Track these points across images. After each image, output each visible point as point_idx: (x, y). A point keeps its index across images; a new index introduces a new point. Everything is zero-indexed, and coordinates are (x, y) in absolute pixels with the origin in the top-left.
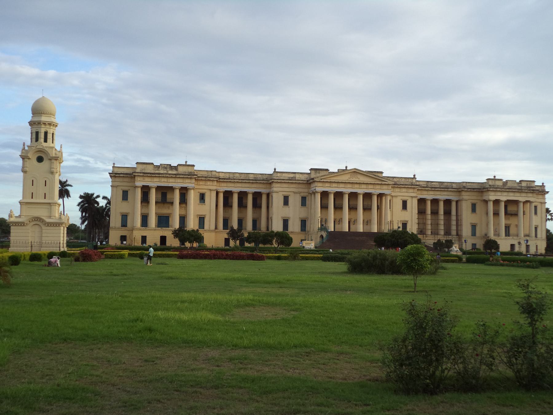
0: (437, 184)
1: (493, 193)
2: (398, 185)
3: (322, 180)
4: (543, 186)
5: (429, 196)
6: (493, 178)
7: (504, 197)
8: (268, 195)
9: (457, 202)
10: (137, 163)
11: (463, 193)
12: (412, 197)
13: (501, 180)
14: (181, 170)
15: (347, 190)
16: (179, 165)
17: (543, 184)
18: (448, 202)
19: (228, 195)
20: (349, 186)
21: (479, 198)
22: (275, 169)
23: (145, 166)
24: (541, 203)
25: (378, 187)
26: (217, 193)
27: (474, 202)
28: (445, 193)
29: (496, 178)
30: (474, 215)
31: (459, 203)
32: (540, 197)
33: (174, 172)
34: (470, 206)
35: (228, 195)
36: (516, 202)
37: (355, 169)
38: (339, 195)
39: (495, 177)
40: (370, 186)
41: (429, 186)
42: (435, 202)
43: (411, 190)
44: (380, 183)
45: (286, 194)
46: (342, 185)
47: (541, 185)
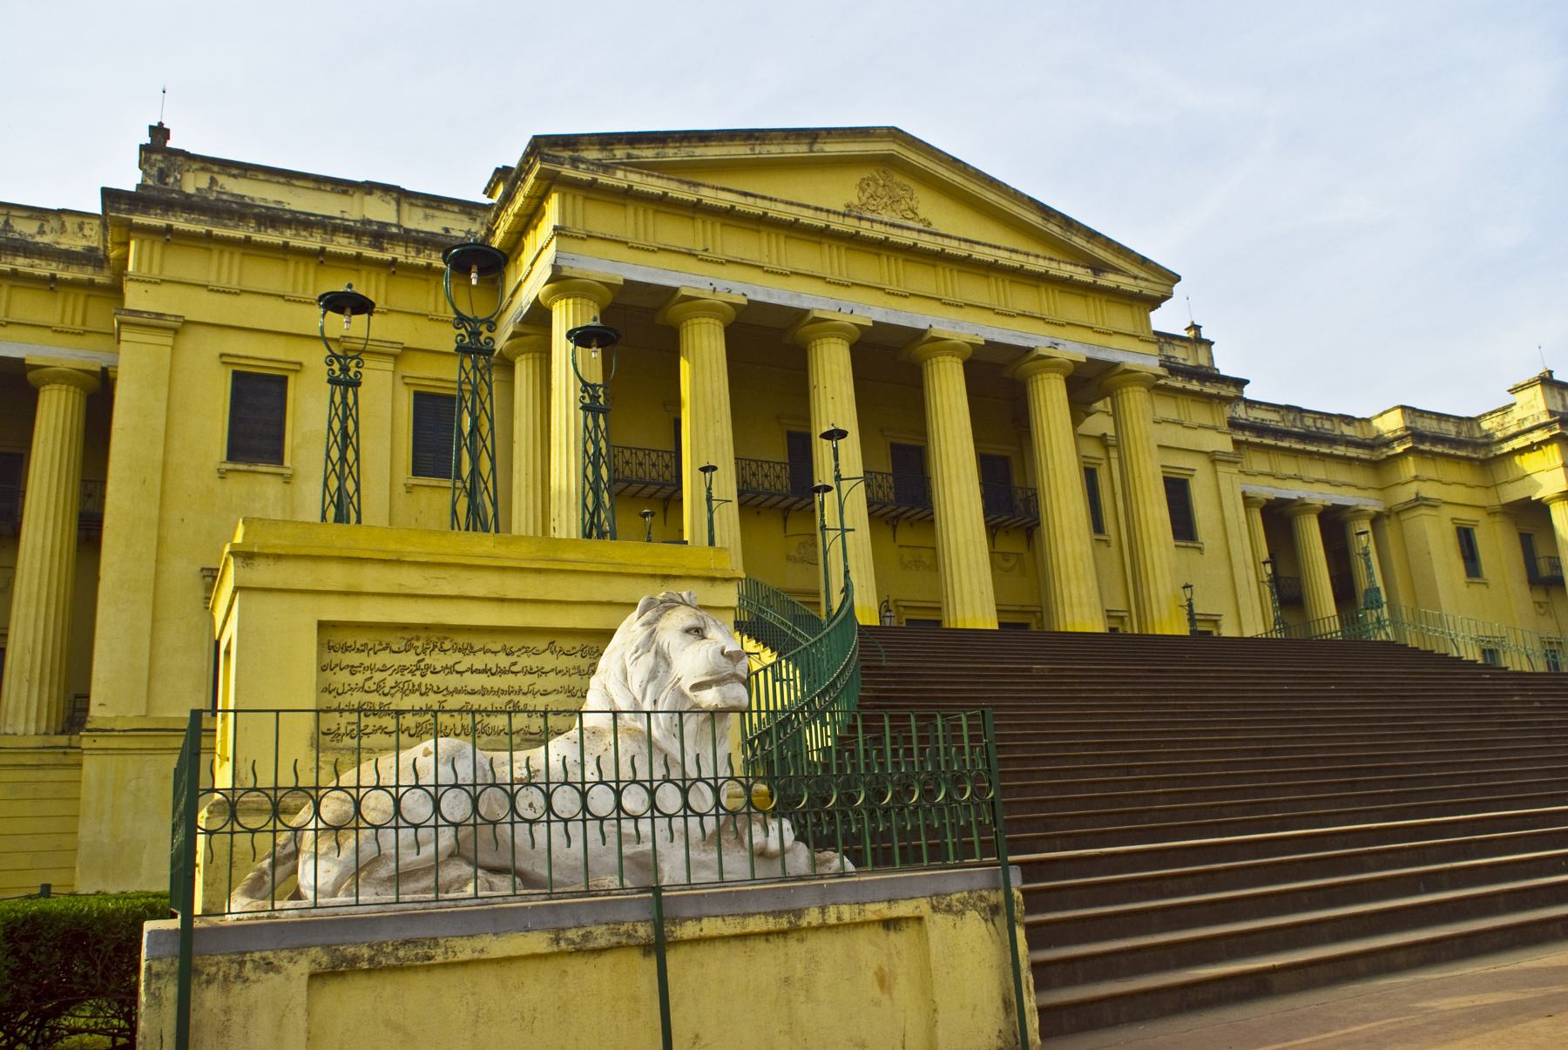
3: (620, 179)
8: (98, 395)
9: (1377, 520)
12: (1214, 458)
15: (843, 299)
20: (865, 268)
21: (1480, 497)
22: (159, 133)
25: (1074, 309)
28: (1317, 471)
31: (1390, 531)
37: (894, 134)
38: (768, 351)
40: (1024, 298)
43: (1200, 414)
44: (1082, 275)
45: (262, 353)
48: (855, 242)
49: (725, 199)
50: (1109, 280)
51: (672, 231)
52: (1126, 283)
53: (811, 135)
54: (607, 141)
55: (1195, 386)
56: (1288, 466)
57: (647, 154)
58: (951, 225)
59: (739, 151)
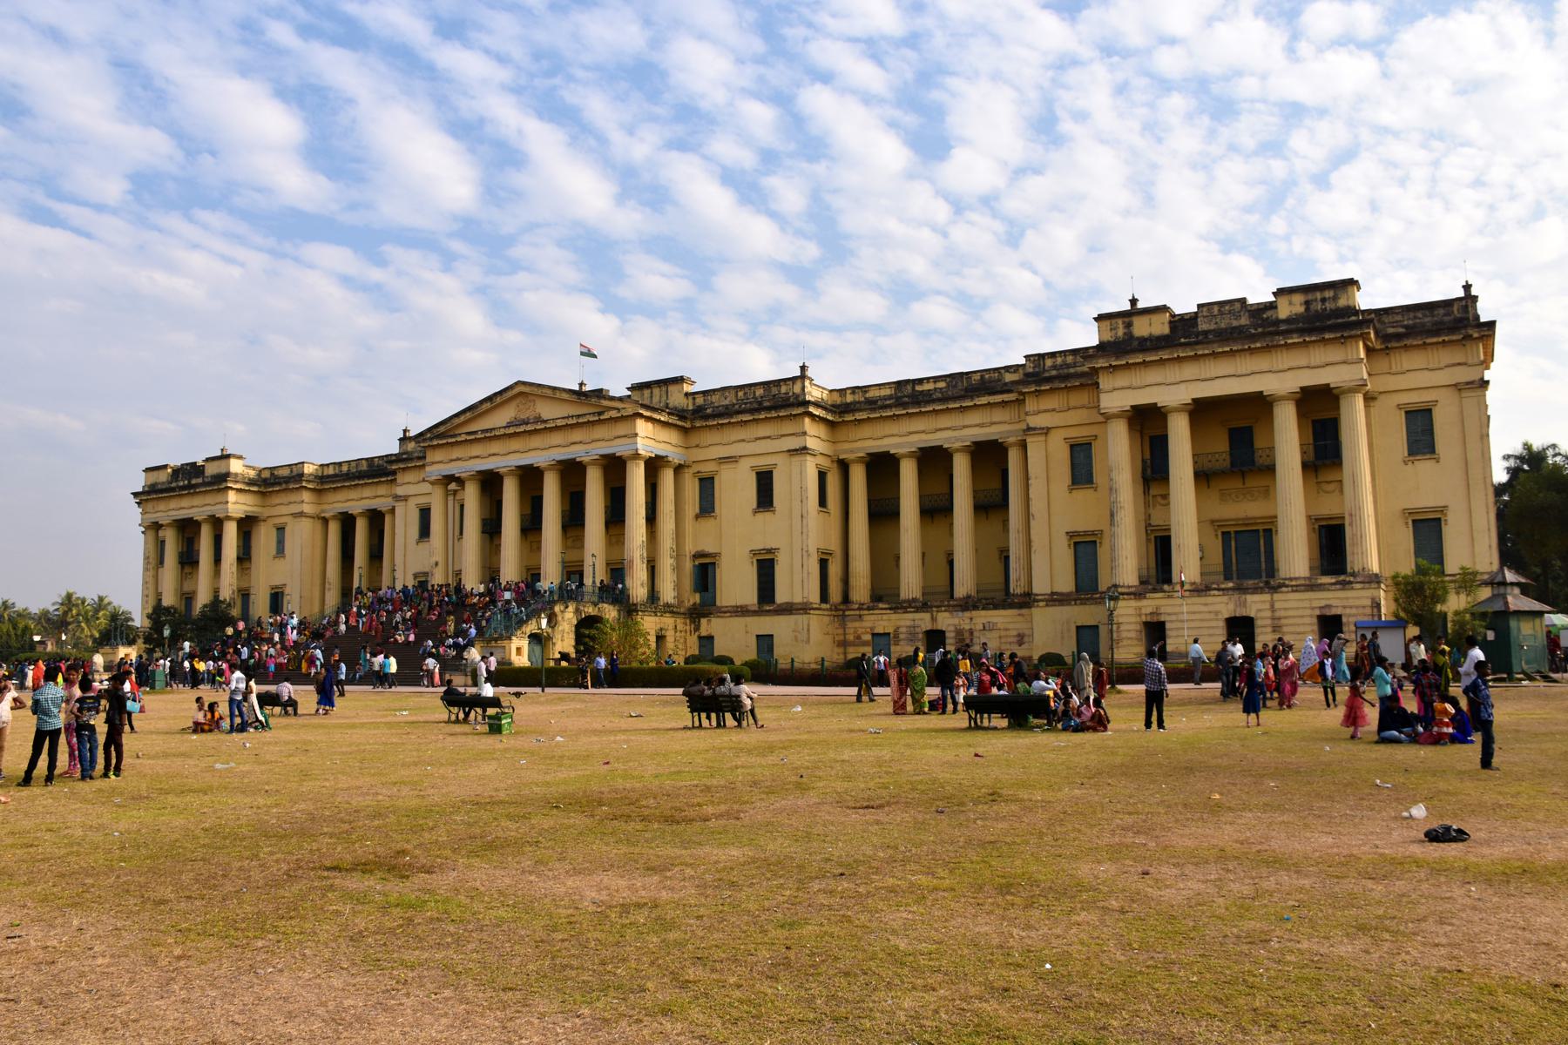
0: (942, 385)
1: (1121, 379)
2: (730, 415)
4: (1470, 298)
5: (901, 437)
6: (1127, 307)
7: (1174, 387)
10: (147, 470)
11: (1031, 405)
13: (1163, 309)
14: (211, 470)
15: (505, 458)
16: (207, 460)
17: (1467, 287)
18: (989, 456)
19: (347, 522)
23: (155, 473)
24: (1458, 387)
26: (325, 521)
27: (1078, 434)
28: (974, 418)
29: (1140, 305)
30: (1083, 495)
32: (1446, 356)
33: (200, 480)
34: (1062, 455)
35: (347, 522)
36: (1260, 404)
37: (519, 383)
39: (1134, 301)
41: (909, 397)
42: (934, 461)
45: (422, 500)
46: (495, 447)
47: (1461, 294)
48: (510, 436)
49: (463, 437)
50: (606, 416)
51: (457, 453)
52: (614, 414)
53: (489, 399)
54: (430, 430)
55: (774, 414)
56: (945, 421)
57: (442, 429)
58: (549, 411)
59: (468, 415)
